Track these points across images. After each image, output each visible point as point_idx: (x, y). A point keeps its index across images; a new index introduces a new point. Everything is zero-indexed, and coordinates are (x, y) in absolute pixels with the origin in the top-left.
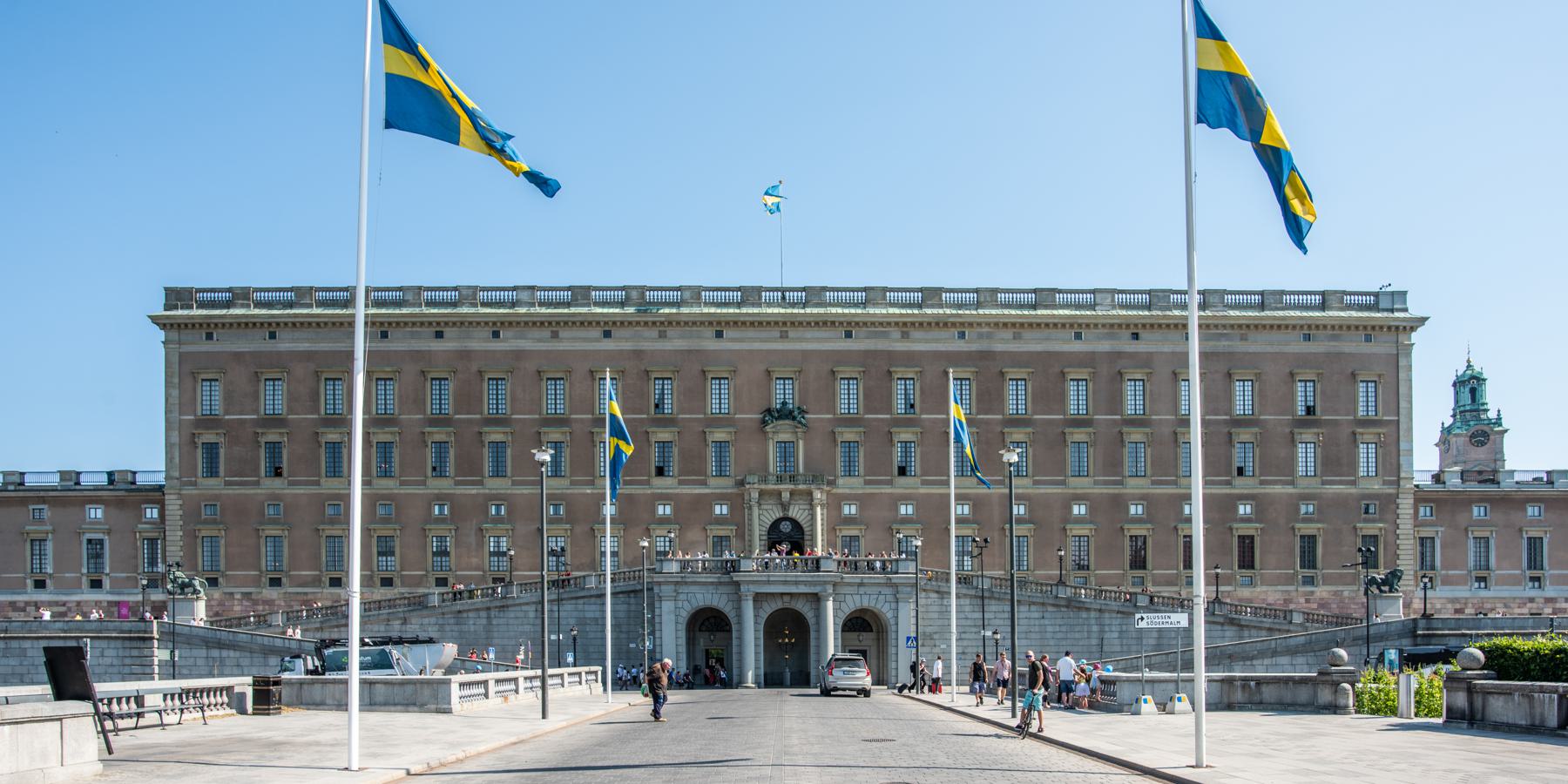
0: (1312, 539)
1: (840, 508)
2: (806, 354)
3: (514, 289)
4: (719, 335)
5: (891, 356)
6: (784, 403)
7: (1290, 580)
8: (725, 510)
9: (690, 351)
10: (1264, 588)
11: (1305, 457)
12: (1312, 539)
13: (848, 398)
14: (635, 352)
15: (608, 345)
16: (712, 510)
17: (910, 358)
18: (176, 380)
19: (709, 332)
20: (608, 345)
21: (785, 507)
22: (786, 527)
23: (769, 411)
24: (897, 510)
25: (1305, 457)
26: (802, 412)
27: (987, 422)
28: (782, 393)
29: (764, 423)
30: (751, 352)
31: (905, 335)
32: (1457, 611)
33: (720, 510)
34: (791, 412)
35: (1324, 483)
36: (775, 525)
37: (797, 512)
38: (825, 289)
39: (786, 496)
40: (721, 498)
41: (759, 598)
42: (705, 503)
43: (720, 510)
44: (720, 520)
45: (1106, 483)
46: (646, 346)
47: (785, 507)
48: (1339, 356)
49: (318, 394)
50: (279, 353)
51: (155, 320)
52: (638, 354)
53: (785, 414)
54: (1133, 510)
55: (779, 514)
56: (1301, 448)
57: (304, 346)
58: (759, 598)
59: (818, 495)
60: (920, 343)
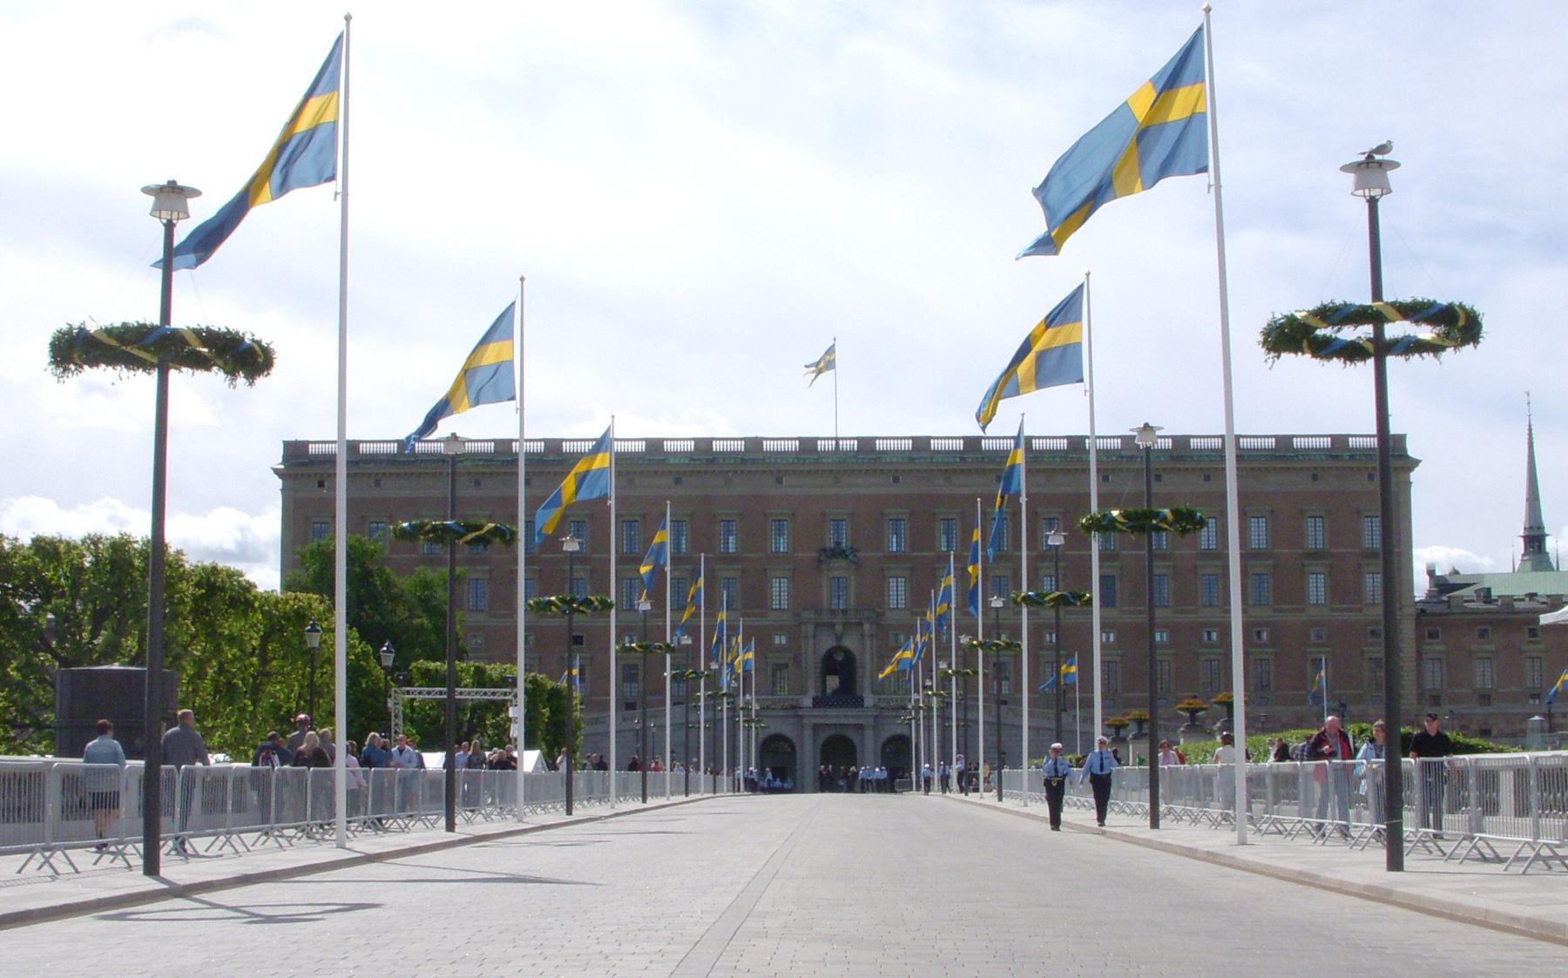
4: (779, 481)
10: (1278, 708)
11: (1316, 587)
21: (839, 638)
23: (824, 550)
25: (1316, 587)
29: (820, 561)
33: (781, 640)
35: (1333, 610)
36: (830, 654)
37: (850, 643)
39: (839, 628)
40: (780, 629)
43: (781, 640)
44: (781, 648)
47: (839, 638)
51: (276, 471)
53: (837, 553)
57: (405, 493)
59: (867, 627)
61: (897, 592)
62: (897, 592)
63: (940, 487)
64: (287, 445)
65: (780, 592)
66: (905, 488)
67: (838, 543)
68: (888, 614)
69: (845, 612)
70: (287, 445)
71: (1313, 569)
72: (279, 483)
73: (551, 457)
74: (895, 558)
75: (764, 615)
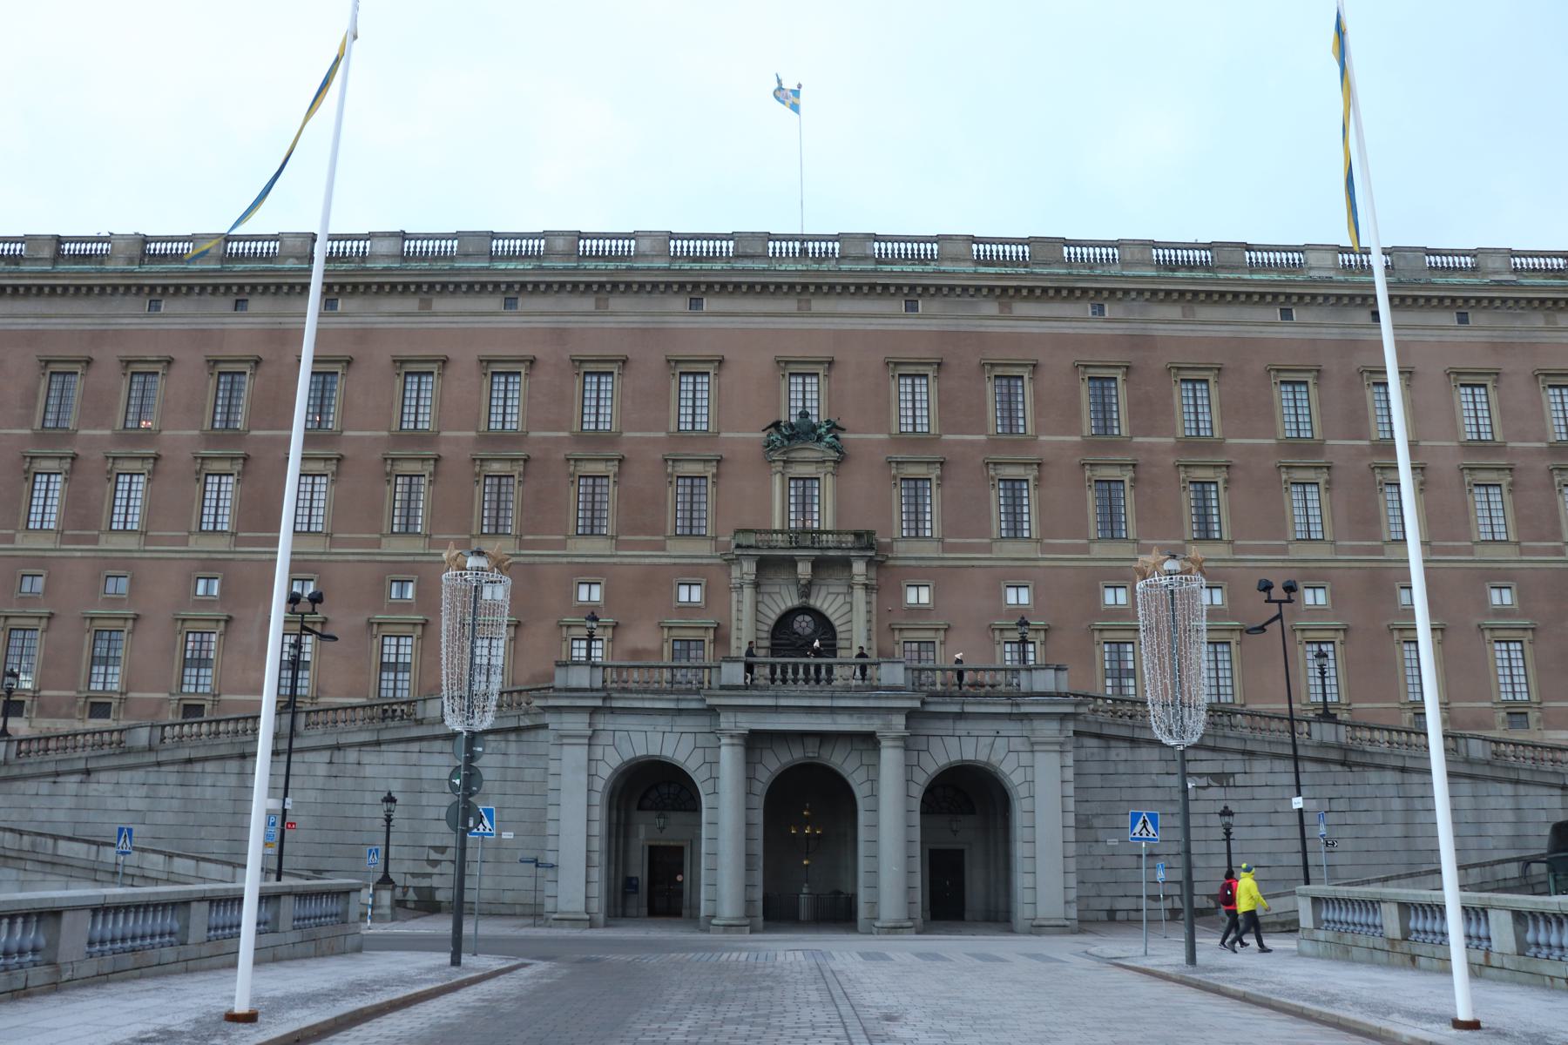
2: (839, 335)
3: (370, 236)
6: (804, 415)
8: (696, 594)
15: (512, 321)
22: (803, 624)
24: (1001, 597)
26: (834, 428)
27: (1150, 449)
33: (691, 595)
34: (814, 428)
40: (690, 573)
41: (754, 742)
42: (659, 581)
43: (691, 595)
45: (1354, 550)
49: (36, 396)
55: (790, 600)
58: (754, 742)
67: (804, 415)
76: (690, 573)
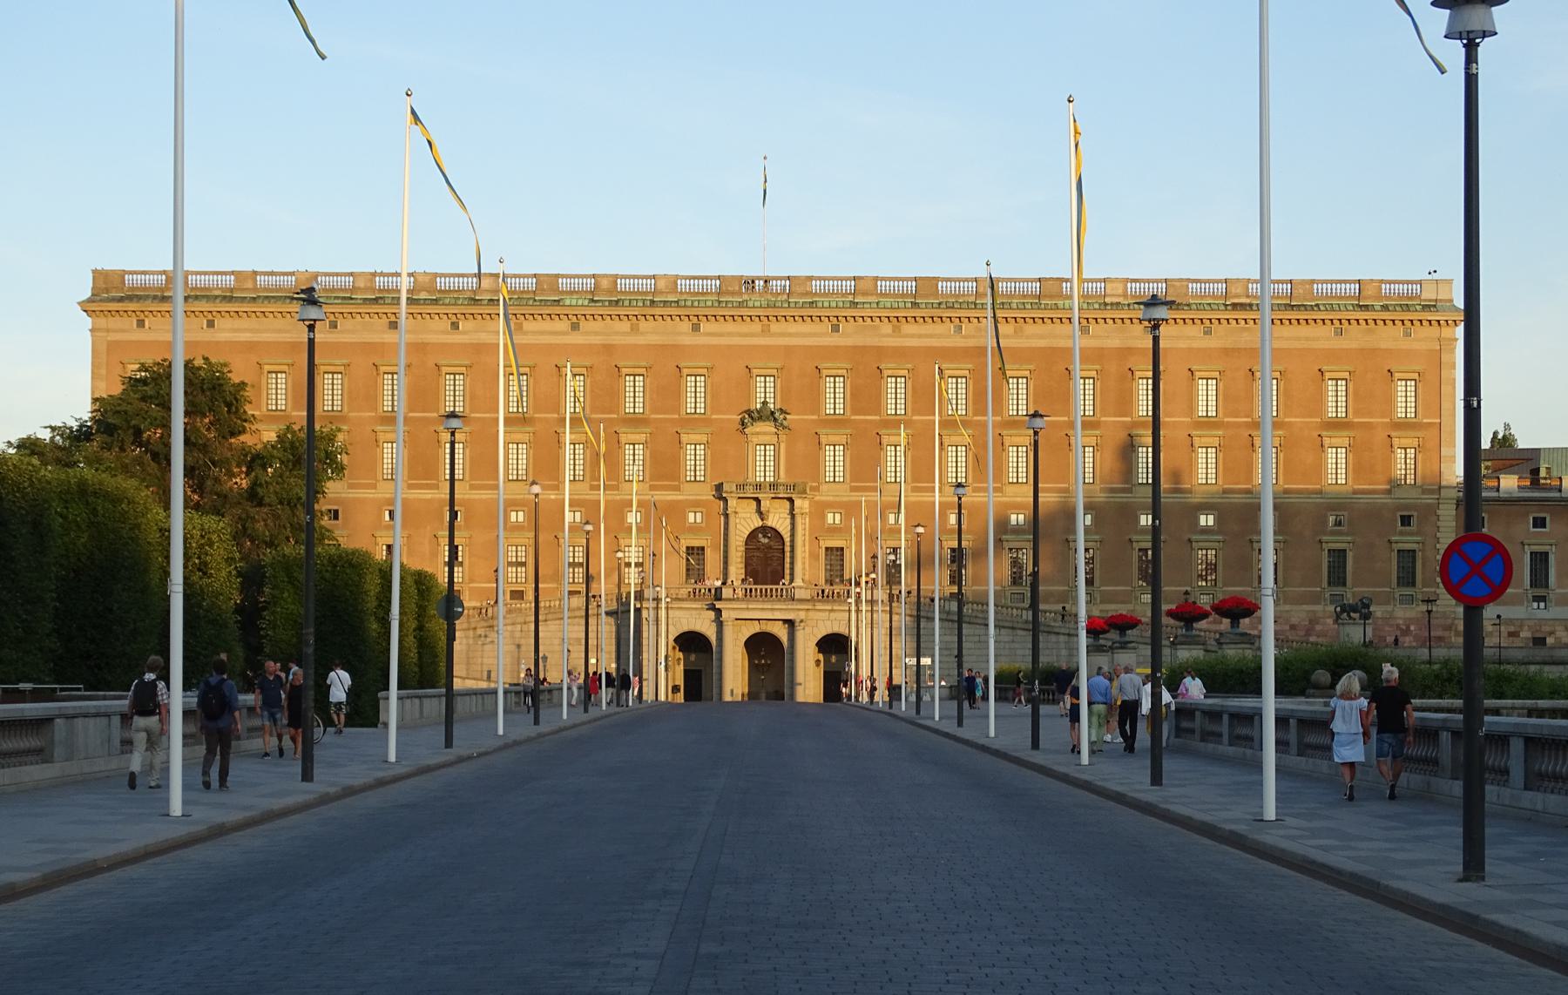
0: (1342, 553)
1: (824, 517)
2: (789, 350)
5: (880, 352)
6: (765, 403)
7: (1315, 599)
9: (663, 346)
10: (1287, 607)
12: (1342, 553)
13: (834, 398)
14: (604, 346)
15: (576, 339)
16: (685, 518)
17: (900, 353)
18: (103, 372)
19: (686, 326)
20: (576, 339)
23: (749, 412)
28: (764, 392)
30: (729, 347)
31: (896, 330)
32: (1511, 634)
36: (753, 536)
37: (778, 519)
38: (810, 278)
42: (675, 511)
44: (694, 529)
46: (617, 340)
48: (1373, 352)
50: (217, 343)
52: (608, 349)
54: (1211, 521)
55: (758, 523)
56: (1331, 452)
60: (916, 336)
61: (834, 462)
62: (834, 462)
63: (885, 336)
64: (97, 274)
65: (694, 458)
66: (850, 336)
67: (765, 403)
68: (824, 488)
69: (773, 486)
70: (97, 274)
71: (1335, 441)
72: (88, 322)
73: (423, 295)
74: (836, 422)
75: (677, 489)
76: (696, 505)
